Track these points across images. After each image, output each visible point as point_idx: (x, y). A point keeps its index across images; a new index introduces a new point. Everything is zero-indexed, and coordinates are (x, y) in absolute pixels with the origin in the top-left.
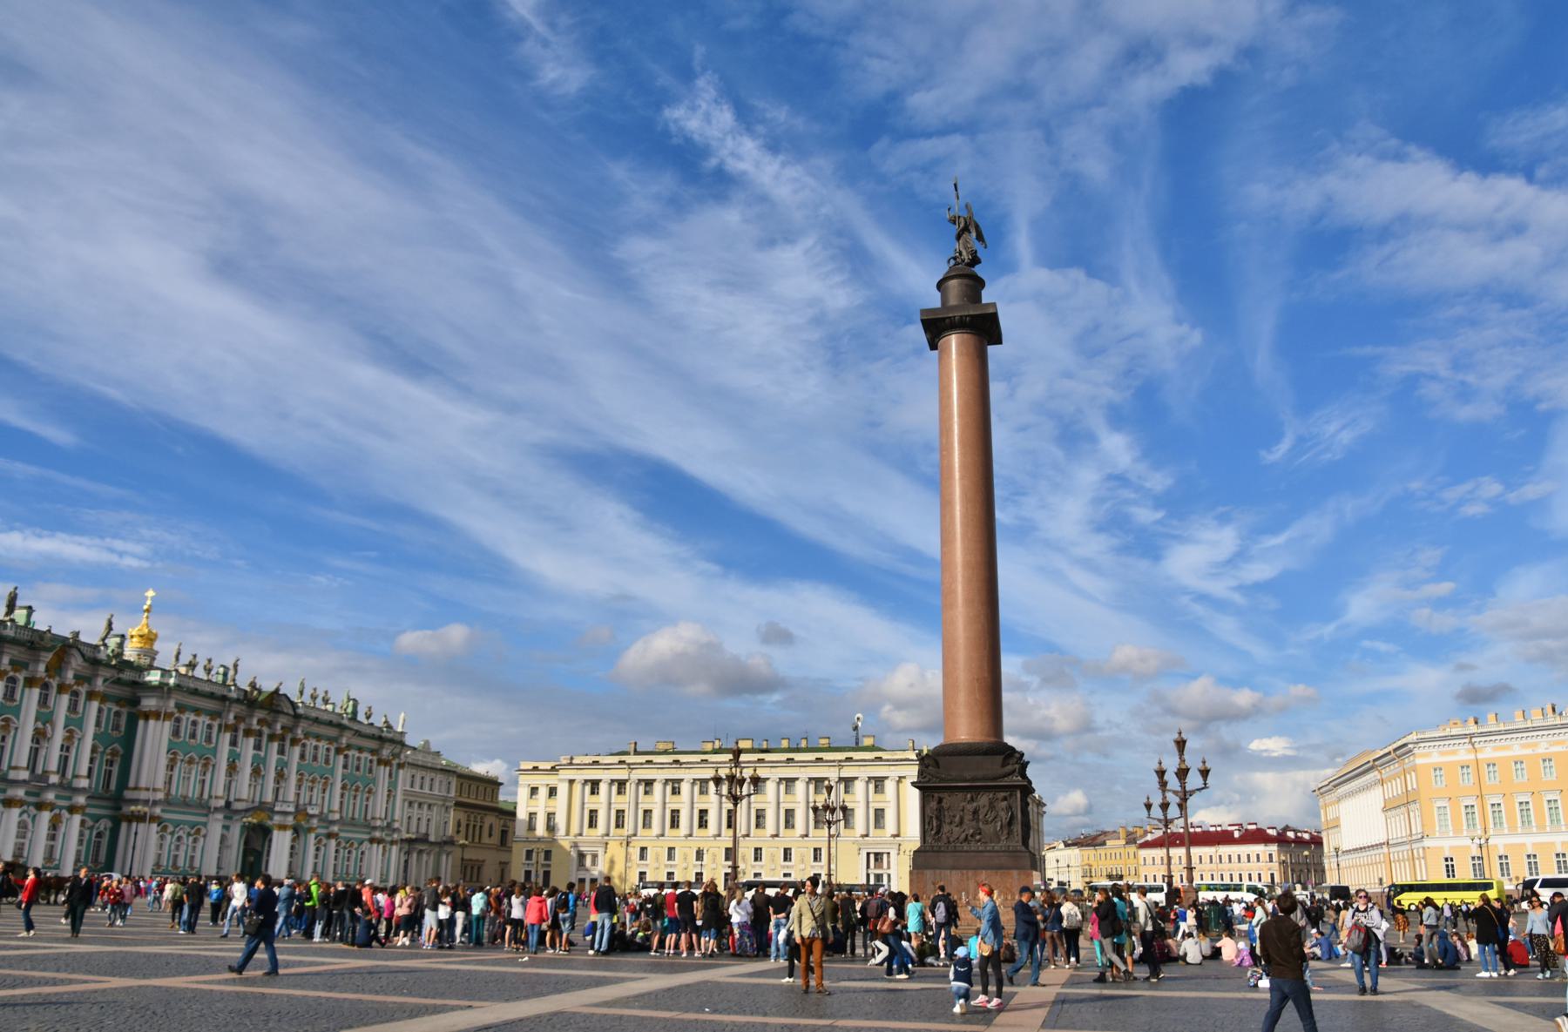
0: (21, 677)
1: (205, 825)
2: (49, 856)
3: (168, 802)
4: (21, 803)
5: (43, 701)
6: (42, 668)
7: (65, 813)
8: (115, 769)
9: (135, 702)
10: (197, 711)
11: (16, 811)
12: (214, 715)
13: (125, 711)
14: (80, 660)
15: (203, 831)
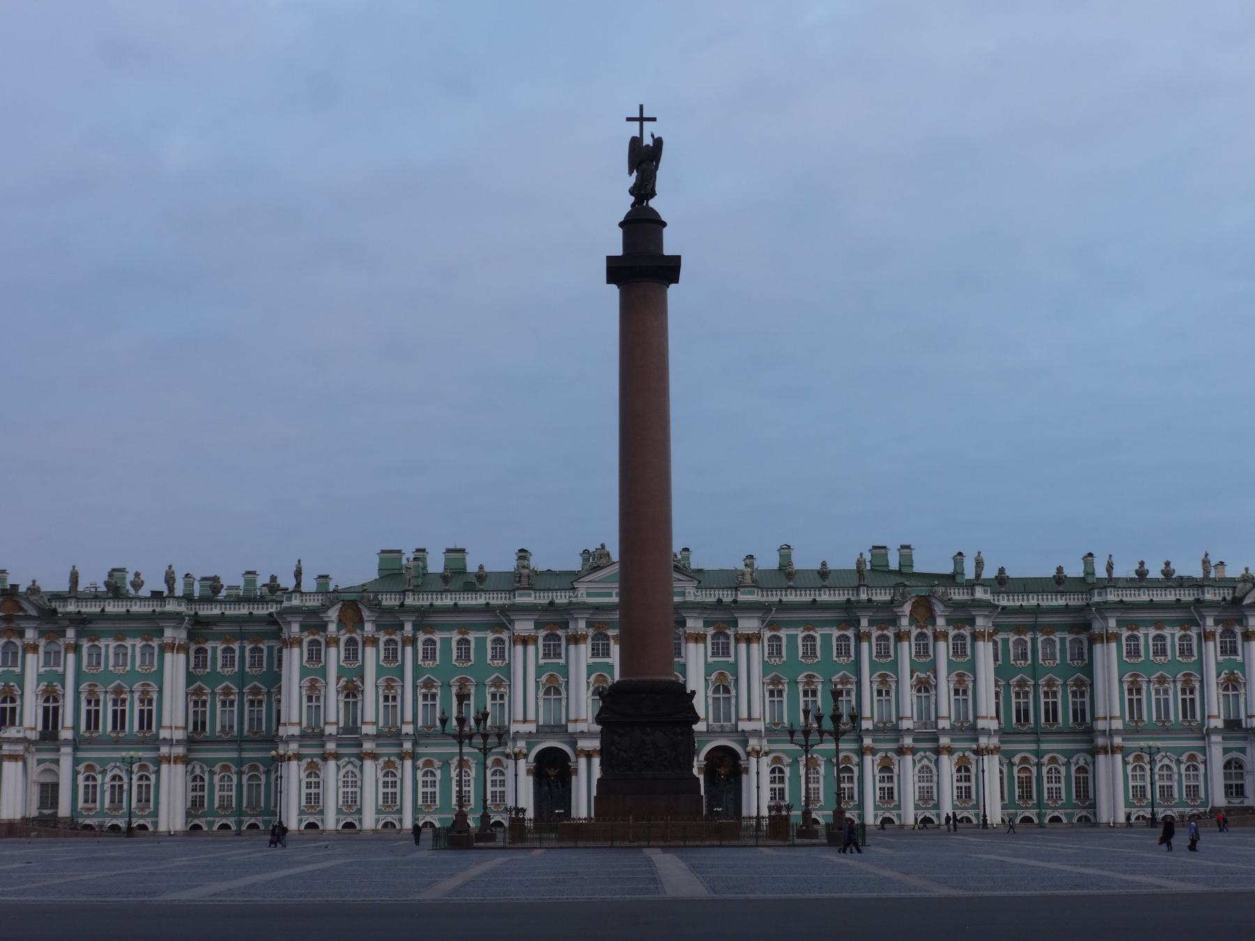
0: (890, 633)
1: (1203, 750)
2: (964, 794)
3: (1126, 732)
4: (913, 751)
5: (923, 651)
6: (905, 622)
7: (973, 757)
8: (1087, 700)
9: (1087, 626)
10: (1159, 624)
11: (909, 758)
12: (1186, 624)
13: (1083, 637)
14: (942, 607)
15: (1200, 757)
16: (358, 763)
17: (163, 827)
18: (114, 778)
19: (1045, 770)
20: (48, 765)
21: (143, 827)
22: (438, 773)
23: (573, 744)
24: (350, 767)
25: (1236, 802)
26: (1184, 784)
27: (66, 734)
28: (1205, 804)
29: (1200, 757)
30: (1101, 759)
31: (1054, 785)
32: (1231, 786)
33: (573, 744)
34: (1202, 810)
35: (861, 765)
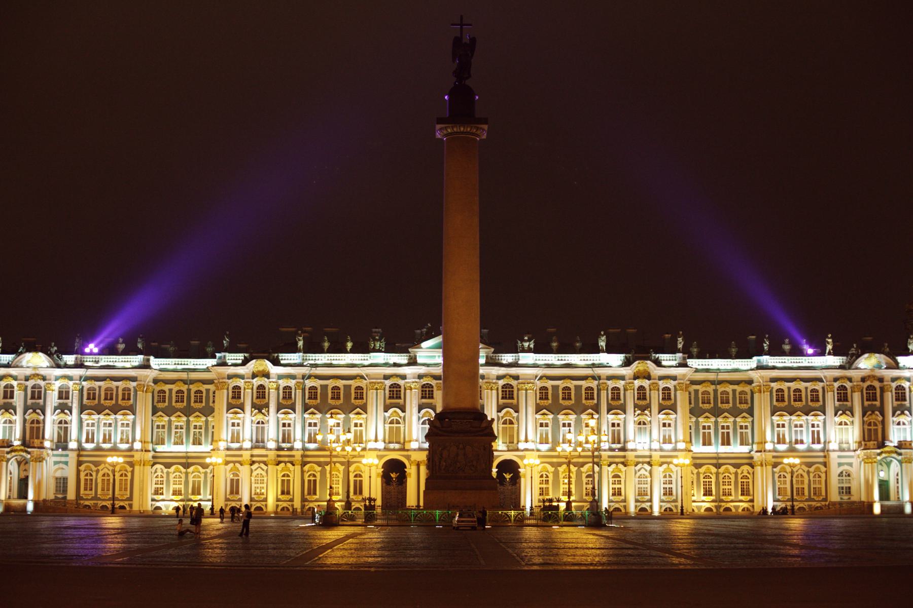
16: (265, 467)
17: (136, 508)
18: (104, 475)
19: (721, 477)
20: (61, 465)
21: (122, 507)
22: (318, 475)
23: (408, 457)
24: (259, 471)
25: (846, 498)
26: (812, 486)
27: (73, 445)
28: (825, 500)
29: (823, 469)
30: (758, 469)
31: (727, 487)
32: (842, 488)
33: (408, 457)
34: (823, 503)
35: (600, 473)
